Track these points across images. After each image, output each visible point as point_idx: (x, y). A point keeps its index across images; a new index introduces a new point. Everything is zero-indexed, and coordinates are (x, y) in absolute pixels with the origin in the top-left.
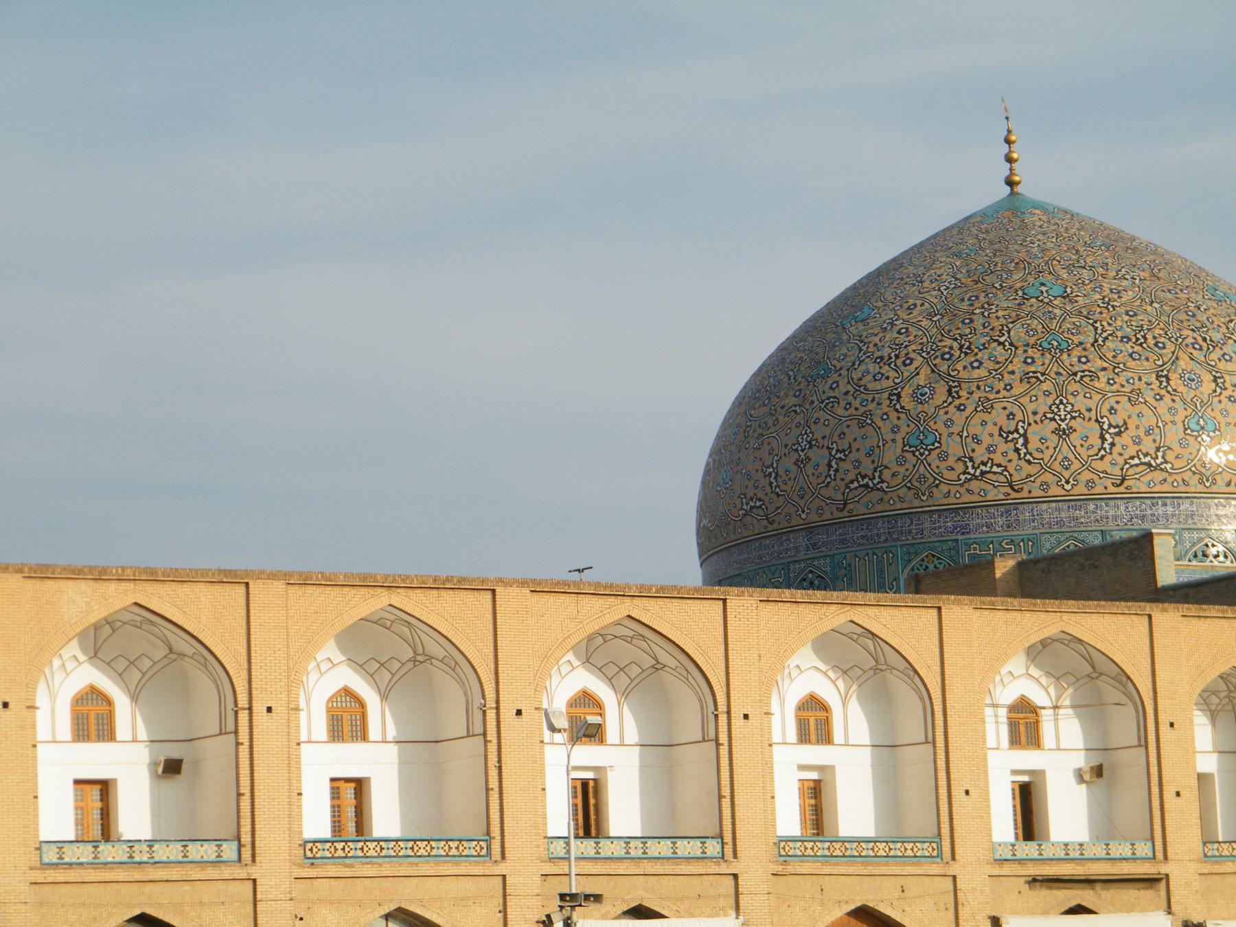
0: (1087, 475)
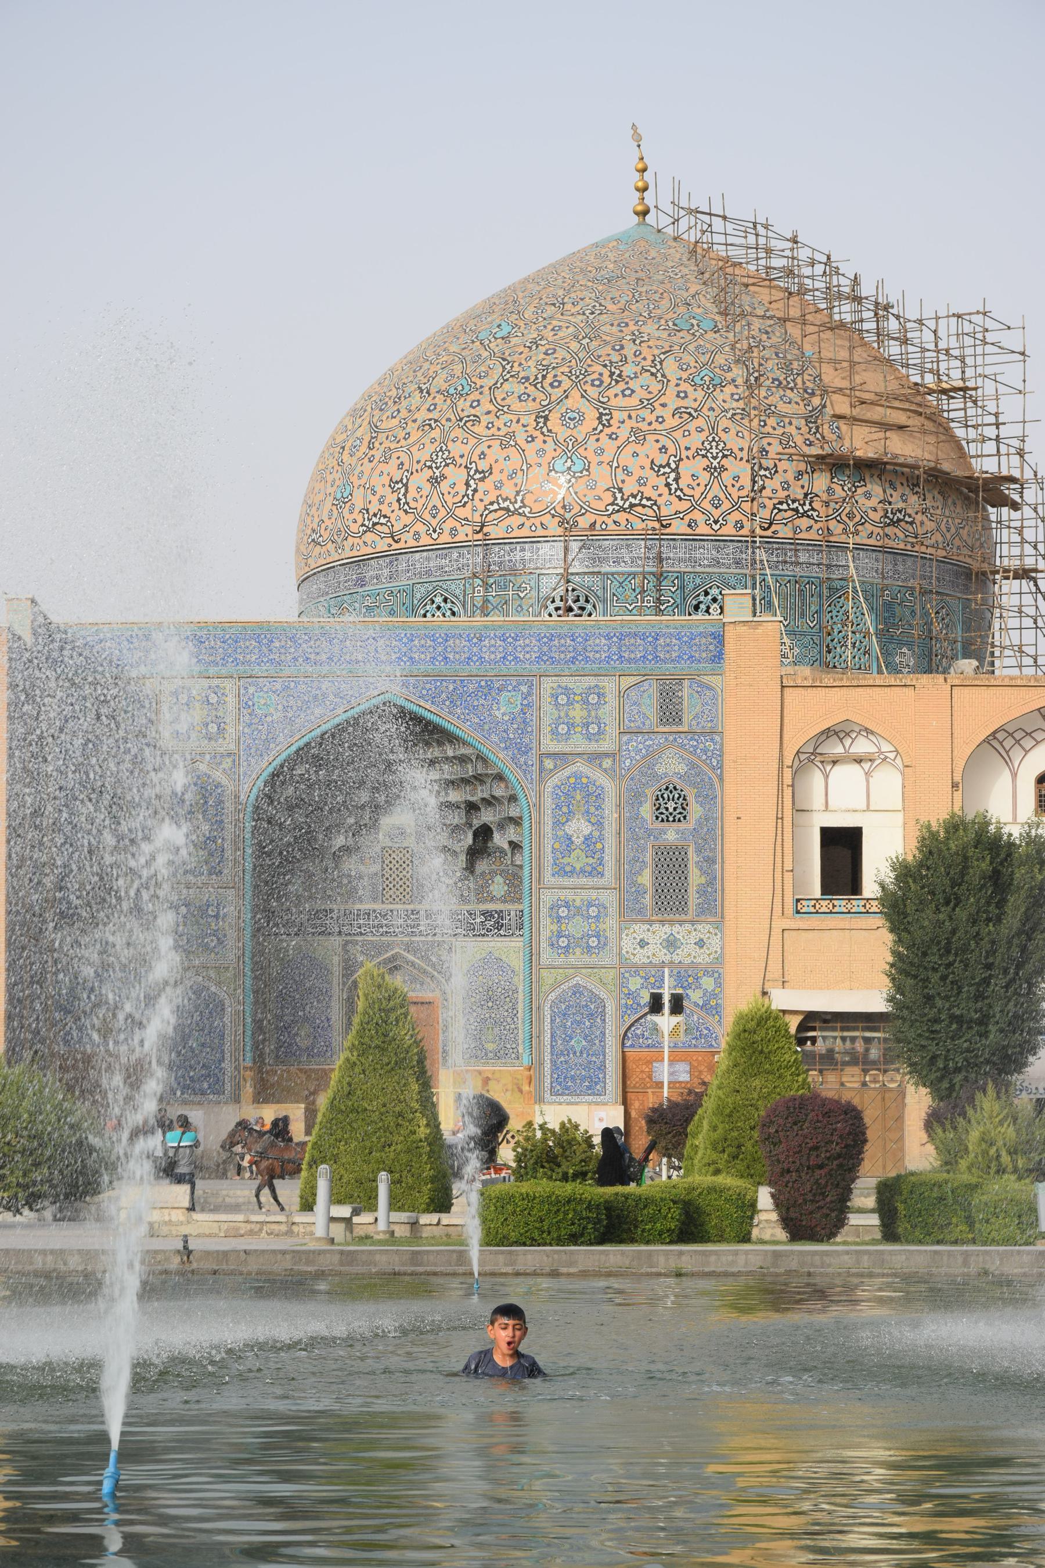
0: (451, 523)
